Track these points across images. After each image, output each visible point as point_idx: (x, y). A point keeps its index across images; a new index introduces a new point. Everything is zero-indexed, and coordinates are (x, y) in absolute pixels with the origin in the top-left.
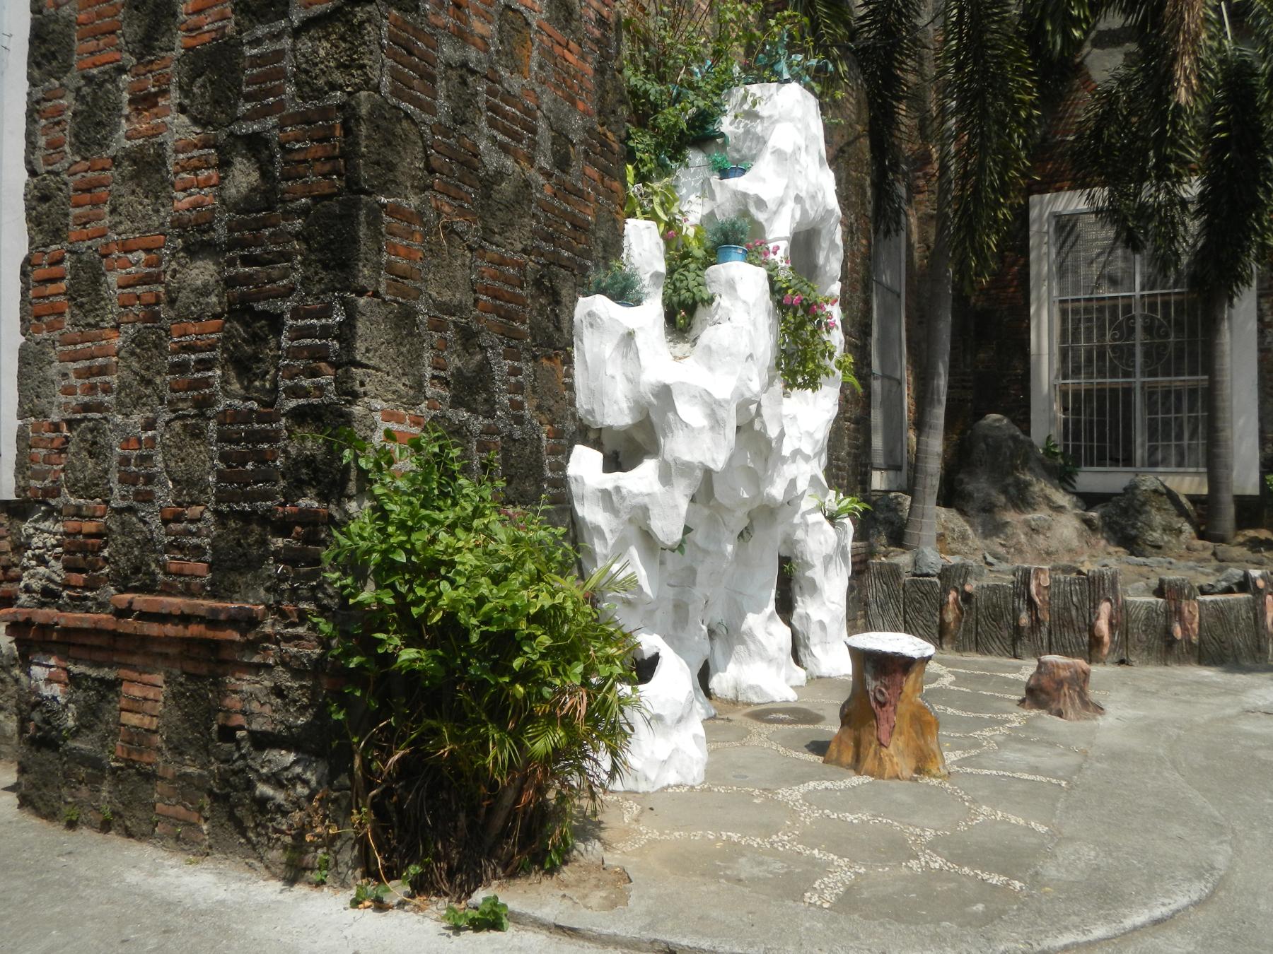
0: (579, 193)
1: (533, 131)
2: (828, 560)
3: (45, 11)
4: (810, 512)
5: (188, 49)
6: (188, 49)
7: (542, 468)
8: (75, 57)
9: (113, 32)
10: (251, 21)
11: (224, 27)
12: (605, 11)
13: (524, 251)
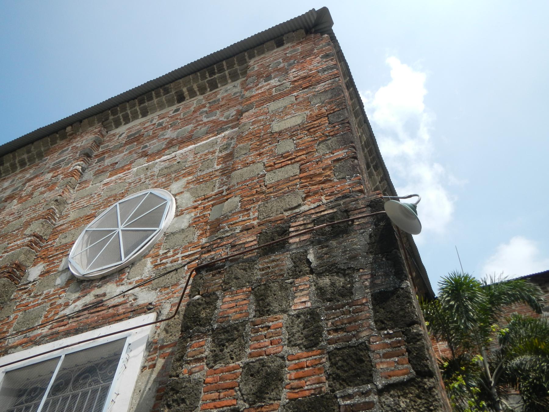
3: (181, 376)
5: (291, 400)
6: (291, 400)
8: (201, 402)
9: (232, 388)
10: (341, 384)
11: (321, 387)
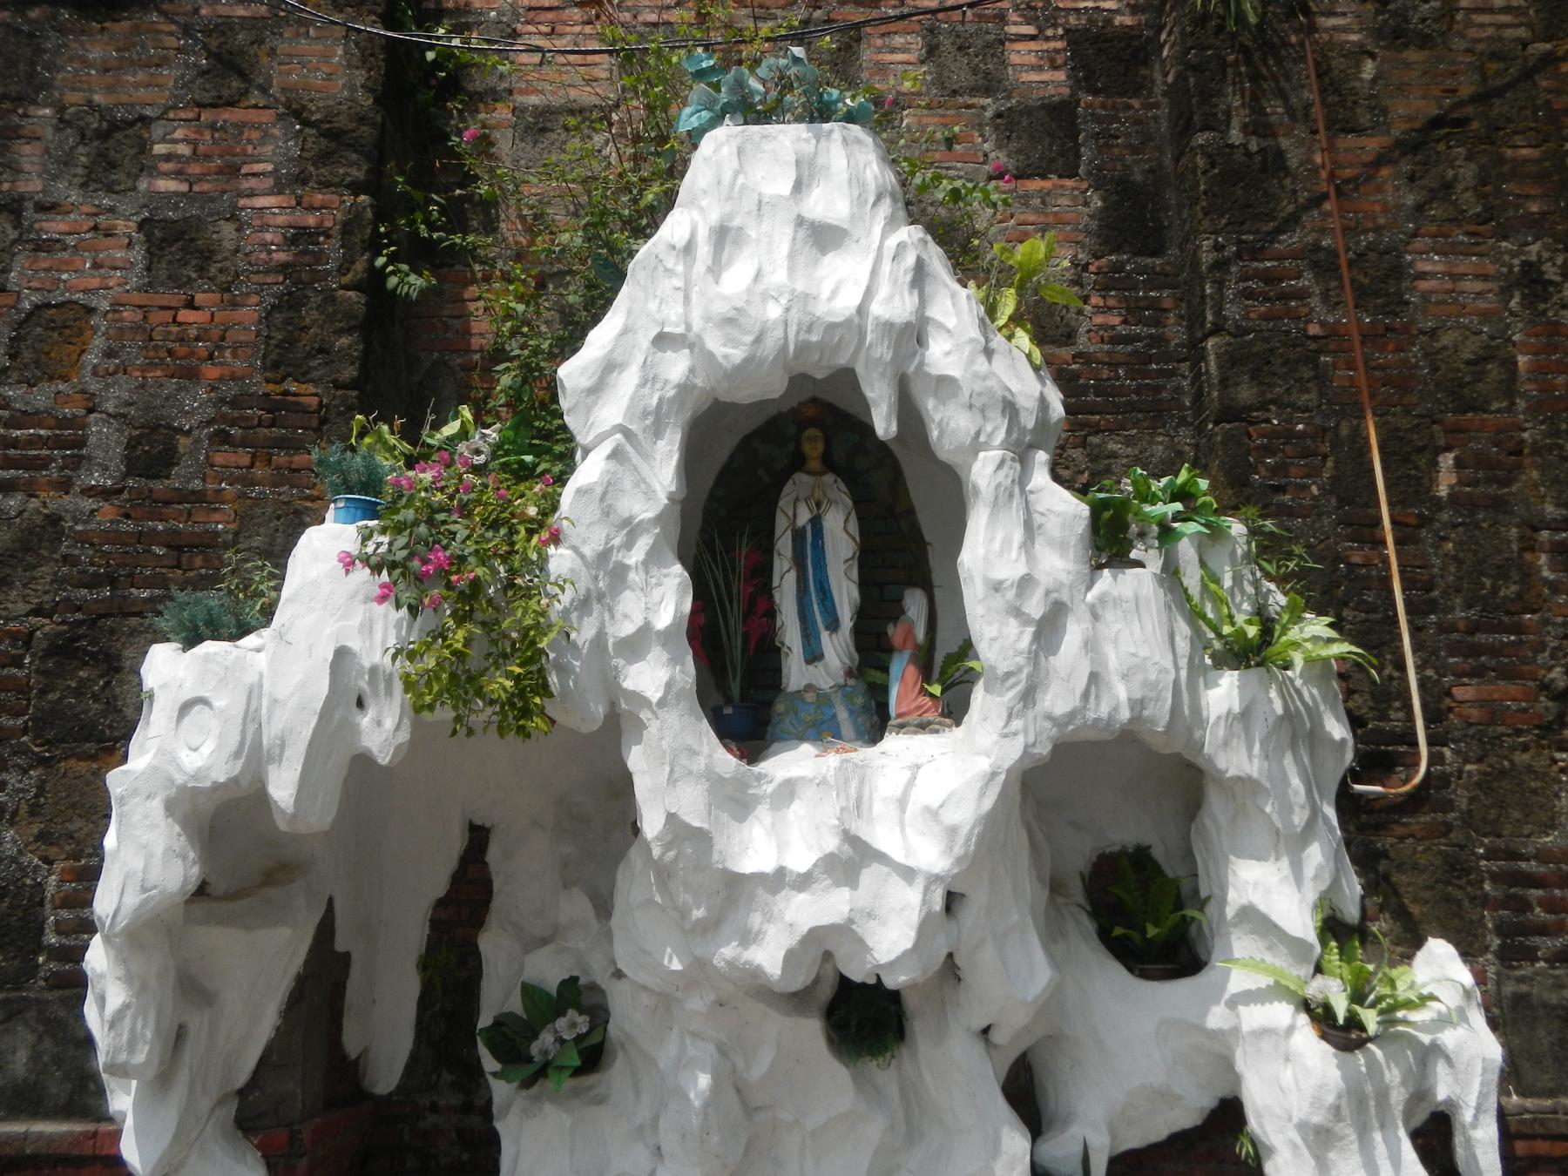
0: (198, 497)
1: (81, 443)
2: (1320, 1139)
4: (1250, 997)
7: (40, 931)
12: (311, 220)
13: (37, 612)
